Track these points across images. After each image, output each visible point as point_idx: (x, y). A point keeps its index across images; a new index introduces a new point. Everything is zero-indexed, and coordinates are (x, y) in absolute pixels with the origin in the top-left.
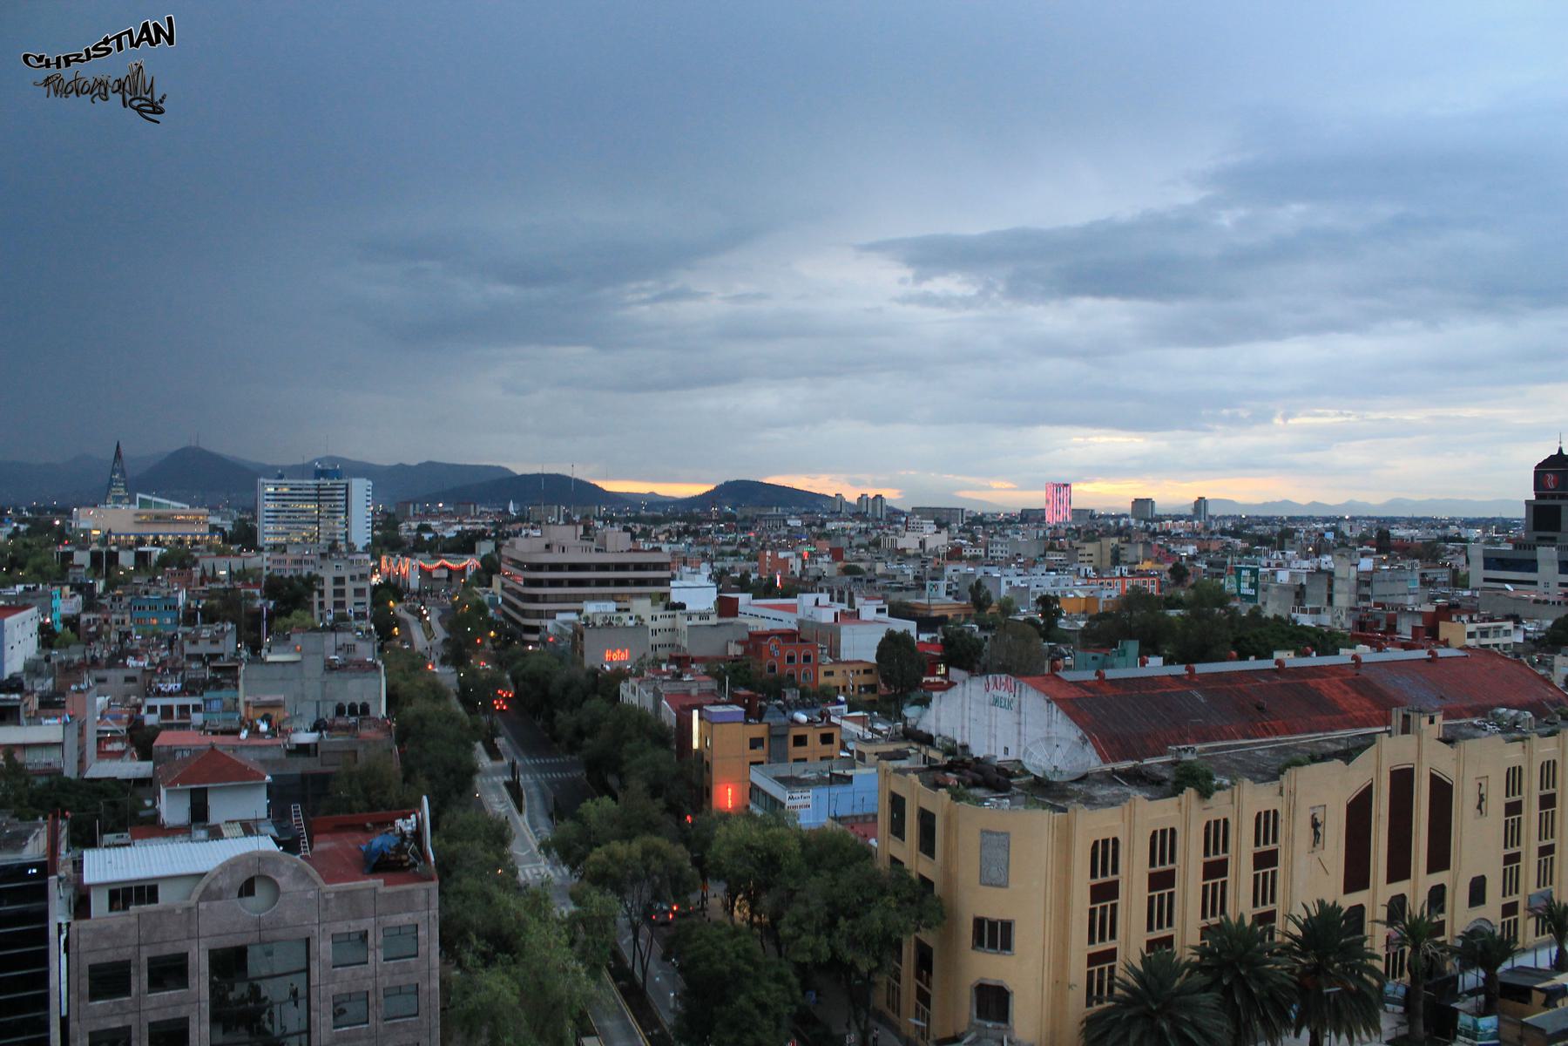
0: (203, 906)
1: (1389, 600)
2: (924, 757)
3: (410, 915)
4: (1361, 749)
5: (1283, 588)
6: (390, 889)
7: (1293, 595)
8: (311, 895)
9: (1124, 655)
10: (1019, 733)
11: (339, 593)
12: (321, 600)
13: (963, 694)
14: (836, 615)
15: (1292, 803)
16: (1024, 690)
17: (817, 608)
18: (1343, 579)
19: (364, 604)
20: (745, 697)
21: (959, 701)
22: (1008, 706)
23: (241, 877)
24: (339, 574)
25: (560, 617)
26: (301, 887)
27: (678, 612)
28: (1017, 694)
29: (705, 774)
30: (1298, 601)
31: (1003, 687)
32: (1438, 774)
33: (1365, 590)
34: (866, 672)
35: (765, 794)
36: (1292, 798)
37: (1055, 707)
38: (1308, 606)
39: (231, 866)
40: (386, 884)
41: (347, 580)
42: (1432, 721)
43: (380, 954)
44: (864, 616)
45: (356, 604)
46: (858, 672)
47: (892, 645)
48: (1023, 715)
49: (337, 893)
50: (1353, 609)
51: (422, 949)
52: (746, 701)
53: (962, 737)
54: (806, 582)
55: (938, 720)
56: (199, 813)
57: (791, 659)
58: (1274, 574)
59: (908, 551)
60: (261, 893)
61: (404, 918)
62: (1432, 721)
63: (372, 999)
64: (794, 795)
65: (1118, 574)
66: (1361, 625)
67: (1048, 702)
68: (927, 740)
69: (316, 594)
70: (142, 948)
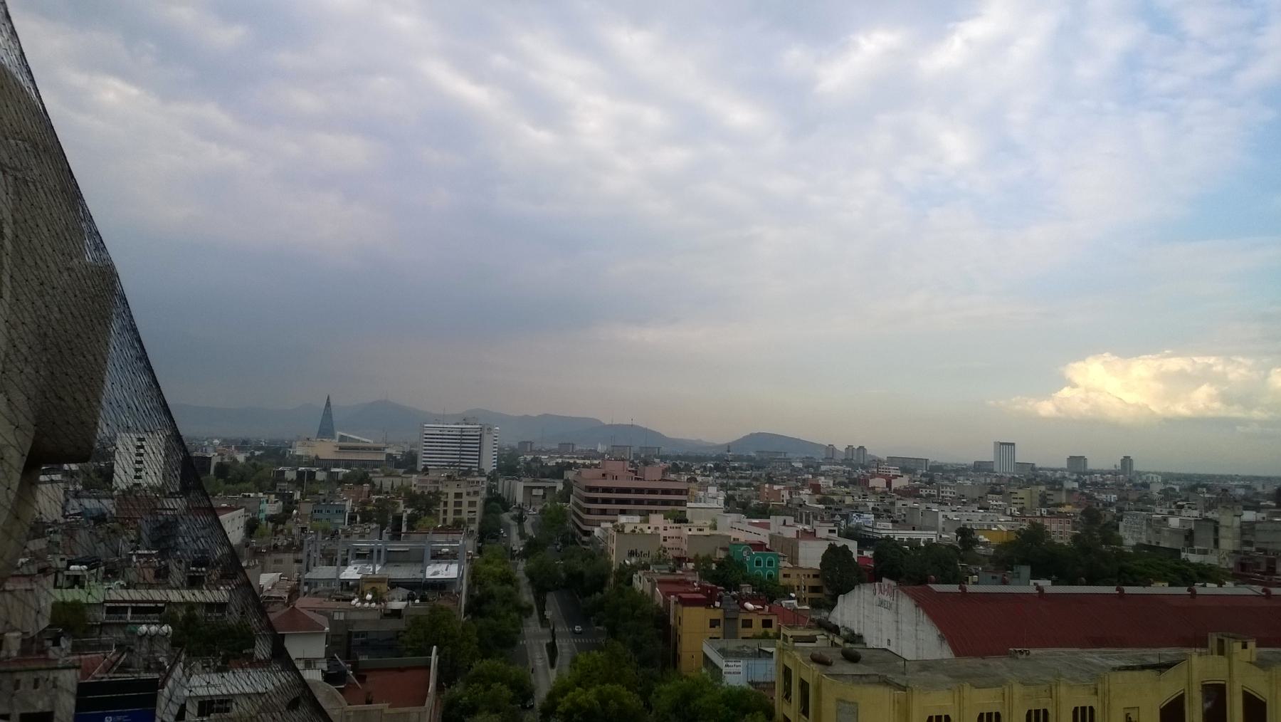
1: (1270, 547)
2: (832, 642)
4: (1168, 666)
5: (1174, 531)
6: (392, 711)
7: (1183, 538)
9: (1019, 577)
10: (897, 629)
11: (458, 504)
12: (445, 508)
13: (859, 597)
14: (798, 532)
15: (1107, 702)
16: (900, 596)
17: (784, 527)
18: (1227, 527)
19: (475, 512)
20: (707, 588)
21: (856, 600)
22: (889, 608)
24: (459, 491)
28: (895, 598)
30: (1187, 542)
31: (886, 593)
32: (1250, 691)
33: (1247, 538)
34: (815, 576)
36: (1107, 698)
37: (921, 612)
38: (1196, 547)
41: (464, 495)
42: (1245, 647)
44: (818, 535)
45: (469, 512)
46: (809, 576)
47: (834, 556)
48: (900, 616)
49: (355, 712)
50: (1234, 552)
52: (709, 591)
53: (859, 629)
55: (842, 615)
57: (758, 563)
58: (1165, 519)
59: (876, 489)
62: (1245, 647)
64: (730, 664)
65: (1038, 514)
66: (1243, 566)
67: (916, 606)
68: (835, 630)
69: (442, 504)
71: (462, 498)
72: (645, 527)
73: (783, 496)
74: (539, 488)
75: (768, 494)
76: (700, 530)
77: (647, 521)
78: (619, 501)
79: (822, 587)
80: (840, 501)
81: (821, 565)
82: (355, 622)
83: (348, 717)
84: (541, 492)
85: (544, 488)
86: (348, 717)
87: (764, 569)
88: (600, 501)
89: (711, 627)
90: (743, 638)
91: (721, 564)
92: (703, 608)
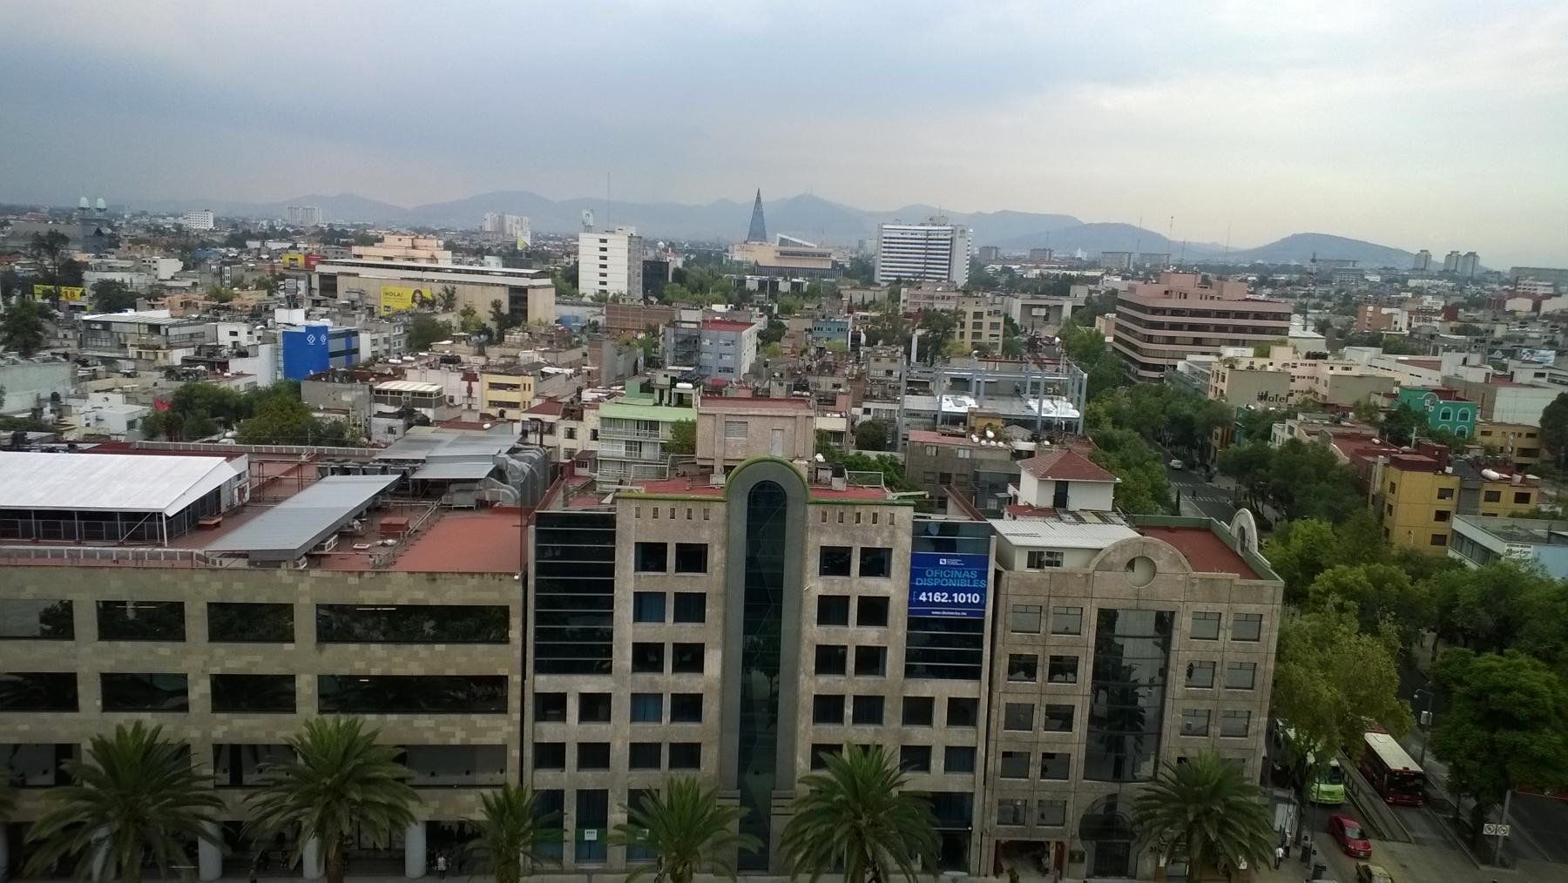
0: (1097, 574)
3: (1258, 606)
8: (1180, 578)
11: (978, 325)
14: (1488, 374)
17: (1464, 367)
20: (1436, 449)
23: (1128, 556)
24: (978, 309)
25: (1190, 358)
26: (1173, 571)
27: (1319, 362)
29: (1387, 516)
34: (1529, 435)
35: (1473, 543)
39: (1122, 546)
40: (1241, 578)
41: (985, 315)
43: (1229, 634)
44: (1518, 378)
45: (991, 335)
49: (1201, 579)
51: (1264, 635)
54: (1418, 340)
56: (1061, 500)
57: (1446, 416)
59: (1518, 314)
60: (1140, 572)
61: (1252, 608)
63: (1218, 669)
64: (1514, 549)
70: (1052, 599)
71: (982, 318)
72: (1259, 362)
73: (1396, 323)
74: (1041, 306)
75: (1370, 319)
76: (1347, 369)
77: (1266, 355)
78: (1193, 327)
79: (1538, 450)
80: (1487, 331)
81: (1542, 421)
82: (982, 461)
83: (1193, 585)
84: (1043, 312)
85: (1047, 307)
86: (1193, 585)
87: (1455, 424)
88: (1230, 329)
89: (1439, 498)
90: (1483, 514)
91: (1391, 416)
92: (1431, 474)
